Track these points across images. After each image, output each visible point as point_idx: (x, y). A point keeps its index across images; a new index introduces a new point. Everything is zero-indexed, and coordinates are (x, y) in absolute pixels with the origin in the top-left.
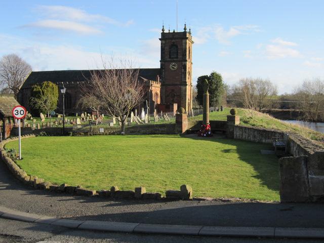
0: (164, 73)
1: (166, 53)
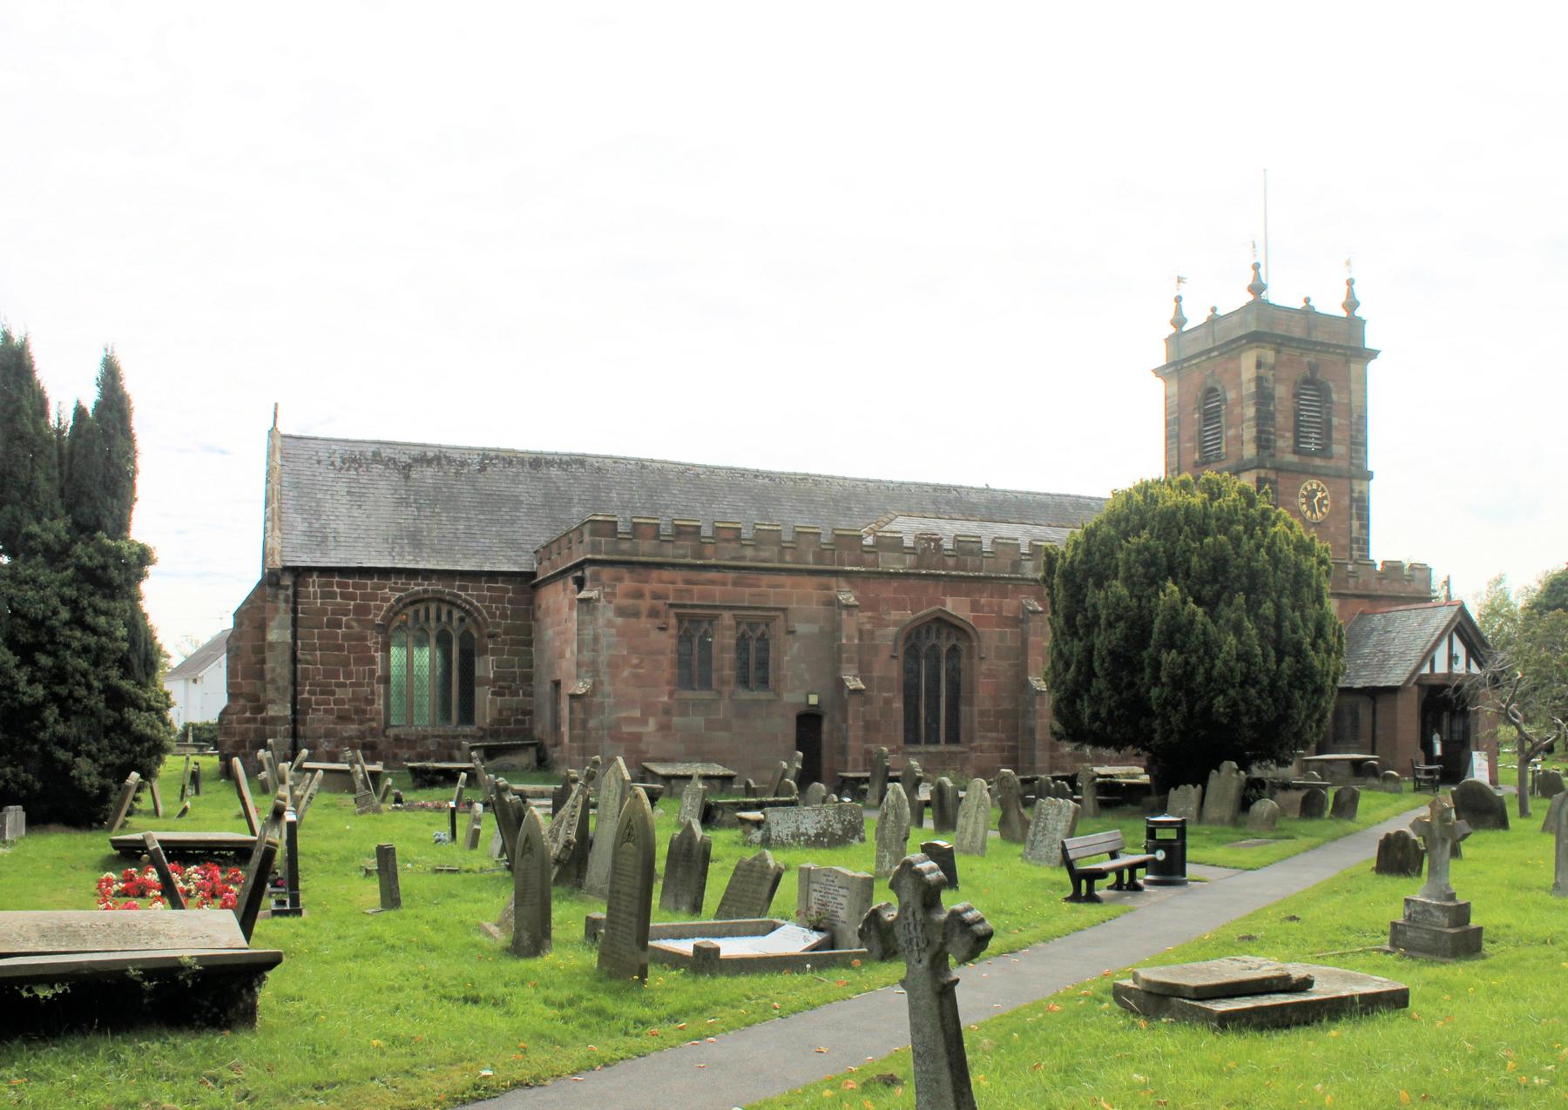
1: (1280, 419)
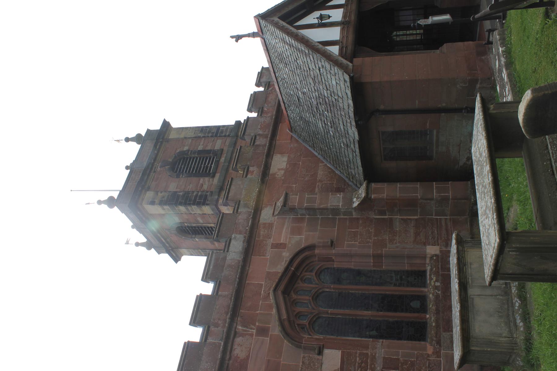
1: (190, 187)
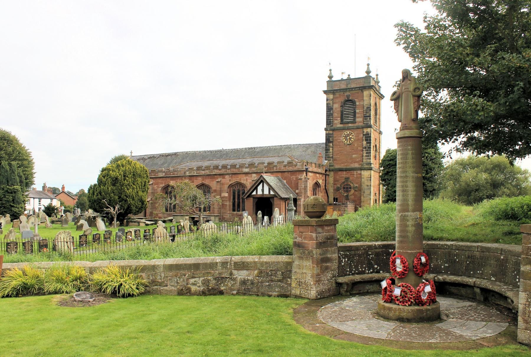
0: (331, 151)
1: (335, 115)
